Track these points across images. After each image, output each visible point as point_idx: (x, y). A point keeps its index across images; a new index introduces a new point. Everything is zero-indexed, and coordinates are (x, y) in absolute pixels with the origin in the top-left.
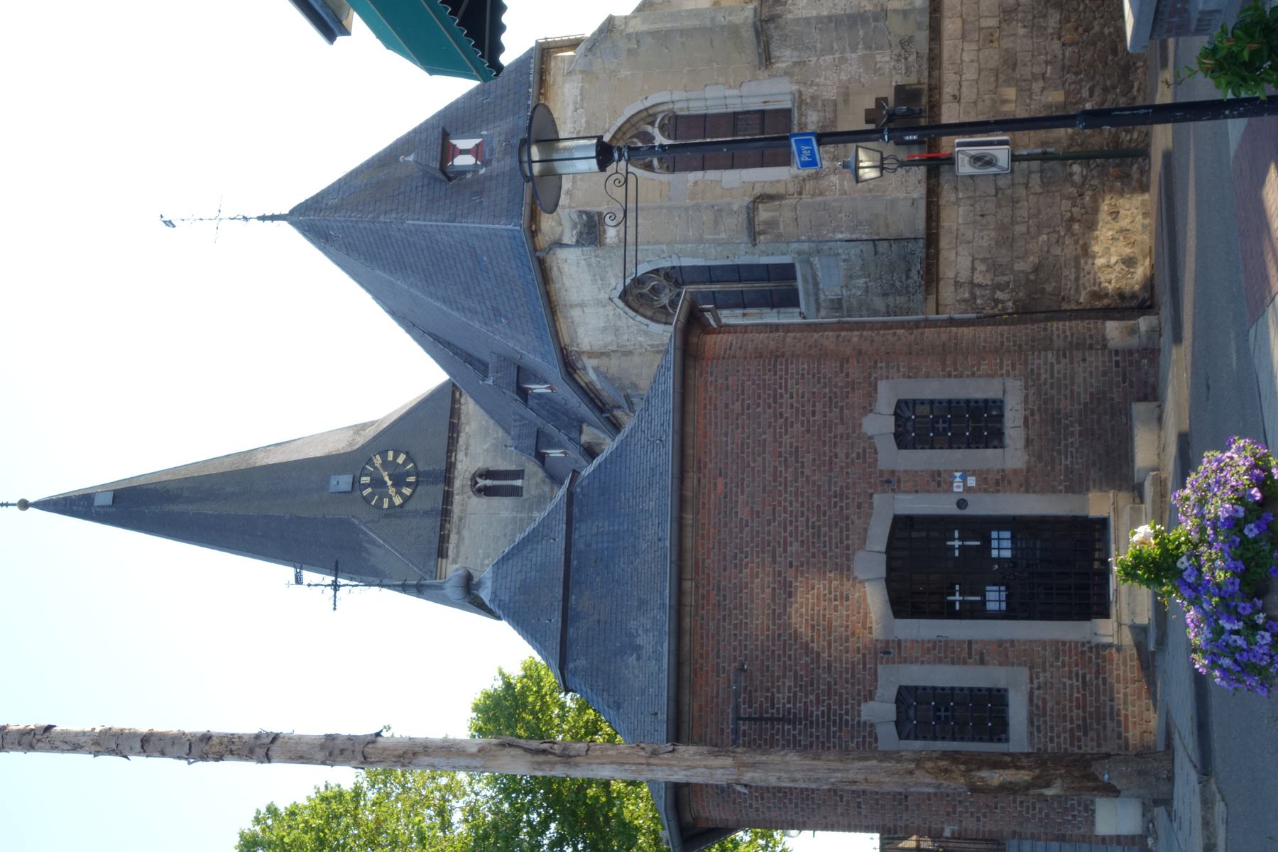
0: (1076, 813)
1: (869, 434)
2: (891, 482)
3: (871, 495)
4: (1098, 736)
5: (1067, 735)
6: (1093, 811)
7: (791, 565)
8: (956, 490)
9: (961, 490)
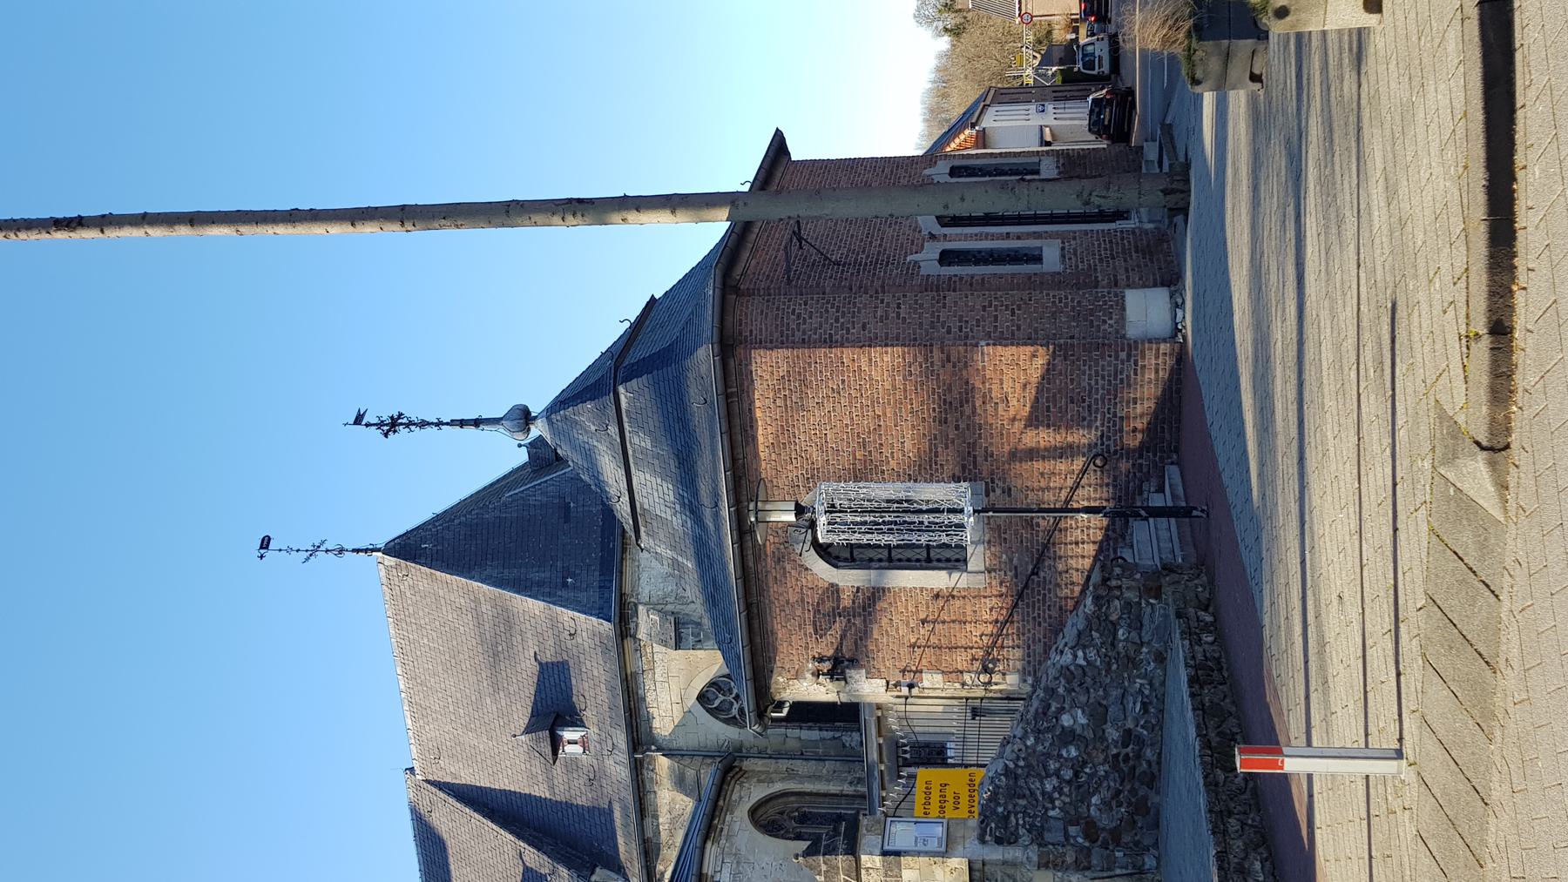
6: (1124, 297)
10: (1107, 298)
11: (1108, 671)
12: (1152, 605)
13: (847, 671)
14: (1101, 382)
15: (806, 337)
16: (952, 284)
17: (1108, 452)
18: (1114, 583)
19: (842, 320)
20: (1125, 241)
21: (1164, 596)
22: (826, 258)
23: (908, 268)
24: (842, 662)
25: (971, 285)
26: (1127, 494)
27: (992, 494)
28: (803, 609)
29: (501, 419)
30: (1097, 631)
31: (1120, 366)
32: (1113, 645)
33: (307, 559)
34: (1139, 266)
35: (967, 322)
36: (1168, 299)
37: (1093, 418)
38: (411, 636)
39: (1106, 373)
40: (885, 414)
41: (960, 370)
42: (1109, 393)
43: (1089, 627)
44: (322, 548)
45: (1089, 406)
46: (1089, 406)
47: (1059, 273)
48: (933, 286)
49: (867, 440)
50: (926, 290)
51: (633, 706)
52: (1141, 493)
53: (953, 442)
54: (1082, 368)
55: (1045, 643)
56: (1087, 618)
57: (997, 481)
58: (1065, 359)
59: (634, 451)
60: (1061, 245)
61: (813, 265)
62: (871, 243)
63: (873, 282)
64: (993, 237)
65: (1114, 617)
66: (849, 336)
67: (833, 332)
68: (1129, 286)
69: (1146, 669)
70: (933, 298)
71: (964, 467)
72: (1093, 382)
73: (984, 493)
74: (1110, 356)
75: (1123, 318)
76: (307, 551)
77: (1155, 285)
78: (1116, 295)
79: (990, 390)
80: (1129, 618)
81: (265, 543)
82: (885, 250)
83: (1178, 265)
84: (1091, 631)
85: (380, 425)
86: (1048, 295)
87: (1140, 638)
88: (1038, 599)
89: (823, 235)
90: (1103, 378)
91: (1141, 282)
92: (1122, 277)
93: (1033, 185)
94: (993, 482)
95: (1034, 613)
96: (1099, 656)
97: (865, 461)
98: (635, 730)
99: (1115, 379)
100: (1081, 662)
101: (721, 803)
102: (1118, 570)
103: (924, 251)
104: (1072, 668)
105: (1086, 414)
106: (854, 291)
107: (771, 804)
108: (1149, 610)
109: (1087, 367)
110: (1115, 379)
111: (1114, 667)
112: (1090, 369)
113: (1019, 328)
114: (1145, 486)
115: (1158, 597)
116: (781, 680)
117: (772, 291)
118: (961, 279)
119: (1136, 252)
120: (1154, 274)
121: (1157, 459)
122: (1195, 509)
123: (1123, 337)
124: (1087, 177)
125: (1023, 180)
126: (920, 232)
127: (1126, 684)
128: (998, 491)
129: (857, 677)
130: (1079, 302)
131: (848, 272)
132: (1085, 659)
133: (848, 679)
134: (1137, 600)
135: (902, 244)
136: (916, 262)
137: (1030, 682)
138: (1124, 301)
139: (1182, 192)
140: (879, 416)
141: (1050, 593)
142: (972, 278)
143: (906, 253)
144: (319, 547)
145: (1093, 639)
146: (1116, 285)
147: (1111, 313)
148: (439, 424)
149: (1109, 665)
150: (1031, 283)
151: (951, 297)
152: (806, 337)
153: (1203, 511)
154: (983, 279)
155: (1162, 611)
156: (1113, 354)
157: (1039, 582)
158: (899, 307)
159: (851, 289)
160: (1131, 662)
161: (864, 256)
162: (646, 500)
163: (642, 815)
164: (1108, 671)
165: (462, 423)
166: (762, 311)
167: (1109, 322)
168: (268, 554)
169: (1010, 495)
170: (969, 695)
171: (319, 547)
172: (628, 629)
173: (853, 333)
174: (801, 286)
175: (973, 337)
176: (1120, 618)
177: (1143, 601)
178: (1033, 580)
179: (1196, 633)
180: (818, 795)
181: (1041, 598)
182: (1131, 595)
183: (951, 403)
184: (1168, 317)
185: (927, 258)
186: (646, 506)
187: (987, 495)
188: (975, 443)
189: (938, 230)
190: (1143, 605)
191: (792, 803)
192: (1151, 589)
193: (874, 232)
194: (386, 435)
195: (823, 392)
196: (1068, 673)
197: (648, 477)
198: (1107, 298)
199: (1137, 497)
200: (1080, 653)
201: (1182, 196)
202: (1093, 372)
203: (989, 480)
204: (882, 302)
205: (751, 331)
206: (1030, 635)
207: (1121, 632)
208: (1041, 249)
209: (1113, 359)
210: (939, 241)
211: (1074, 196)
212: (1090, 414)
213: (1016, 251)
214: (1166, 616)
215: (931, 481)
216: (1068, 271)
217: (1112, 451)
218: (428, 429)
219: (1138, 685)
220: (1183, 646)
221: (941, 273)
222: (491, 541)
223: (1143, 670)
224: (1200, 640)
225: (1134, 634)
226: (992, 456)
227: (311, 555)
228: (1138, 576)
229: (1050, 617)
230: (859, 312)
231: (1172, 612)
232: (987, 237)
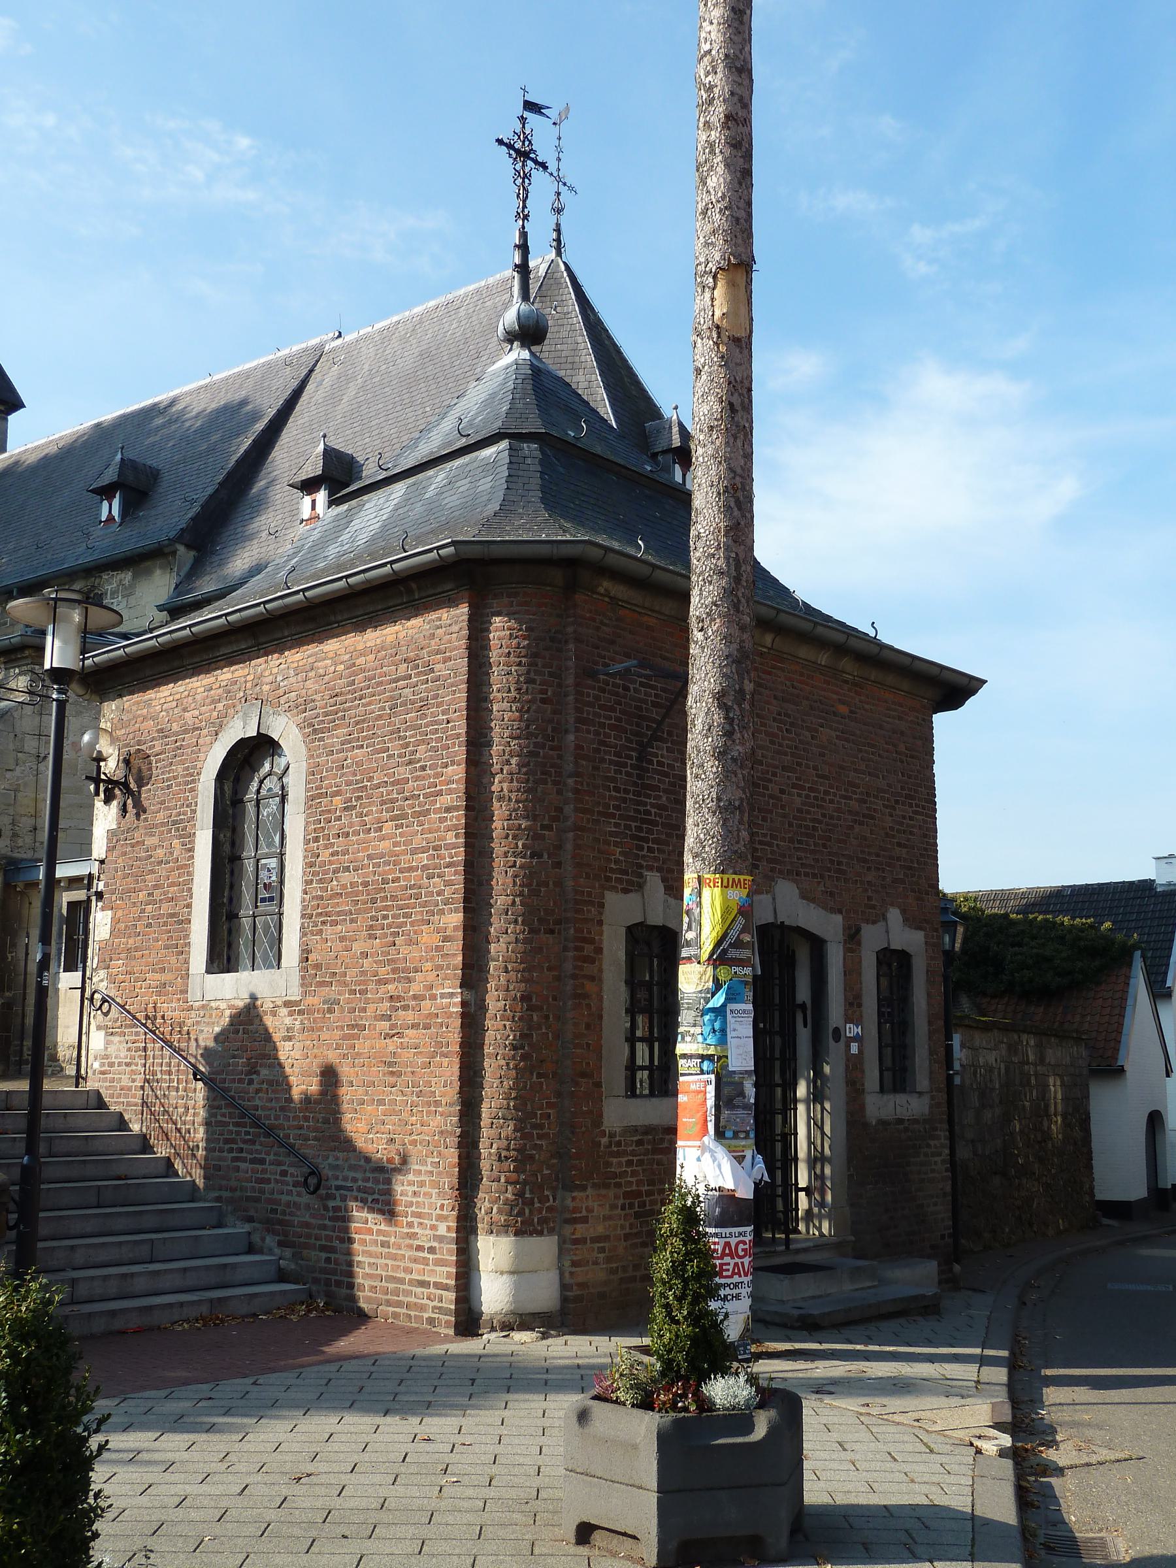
0: (537, 1205)
1: (889, 915)
2: (852, 937)
3: (840, 912)
4: (636, 1235)
5: (634, 1188)
6: (540, 1233)
7: (782, 792)
8: (848, 1026)
9: (848, 1035)
14: (410, 1189)
37: (368, 1175)
40: (382, 839)
54: (429, 1160)
58: (441, 1132)
71: (318, 966)
73: (288, 998)
74: (442, 1206)
77: (564, 1287)
79: (405, 1008)
86: (550, 1105)
92: (581, 1230)
94: (301, 1012)
97: (329, 811)
109: (429, 1168)
128: (288, 1021)
130: (532, 1157)
140: (380, 829)
142: (592, 978)
156: (445, 1213)
187: (287, 1004)
188: (345, 984)
195: (412, 736)
198: (537, 1205)
215: (303, 916)
221: (605, 927)
226: (330, 1011)
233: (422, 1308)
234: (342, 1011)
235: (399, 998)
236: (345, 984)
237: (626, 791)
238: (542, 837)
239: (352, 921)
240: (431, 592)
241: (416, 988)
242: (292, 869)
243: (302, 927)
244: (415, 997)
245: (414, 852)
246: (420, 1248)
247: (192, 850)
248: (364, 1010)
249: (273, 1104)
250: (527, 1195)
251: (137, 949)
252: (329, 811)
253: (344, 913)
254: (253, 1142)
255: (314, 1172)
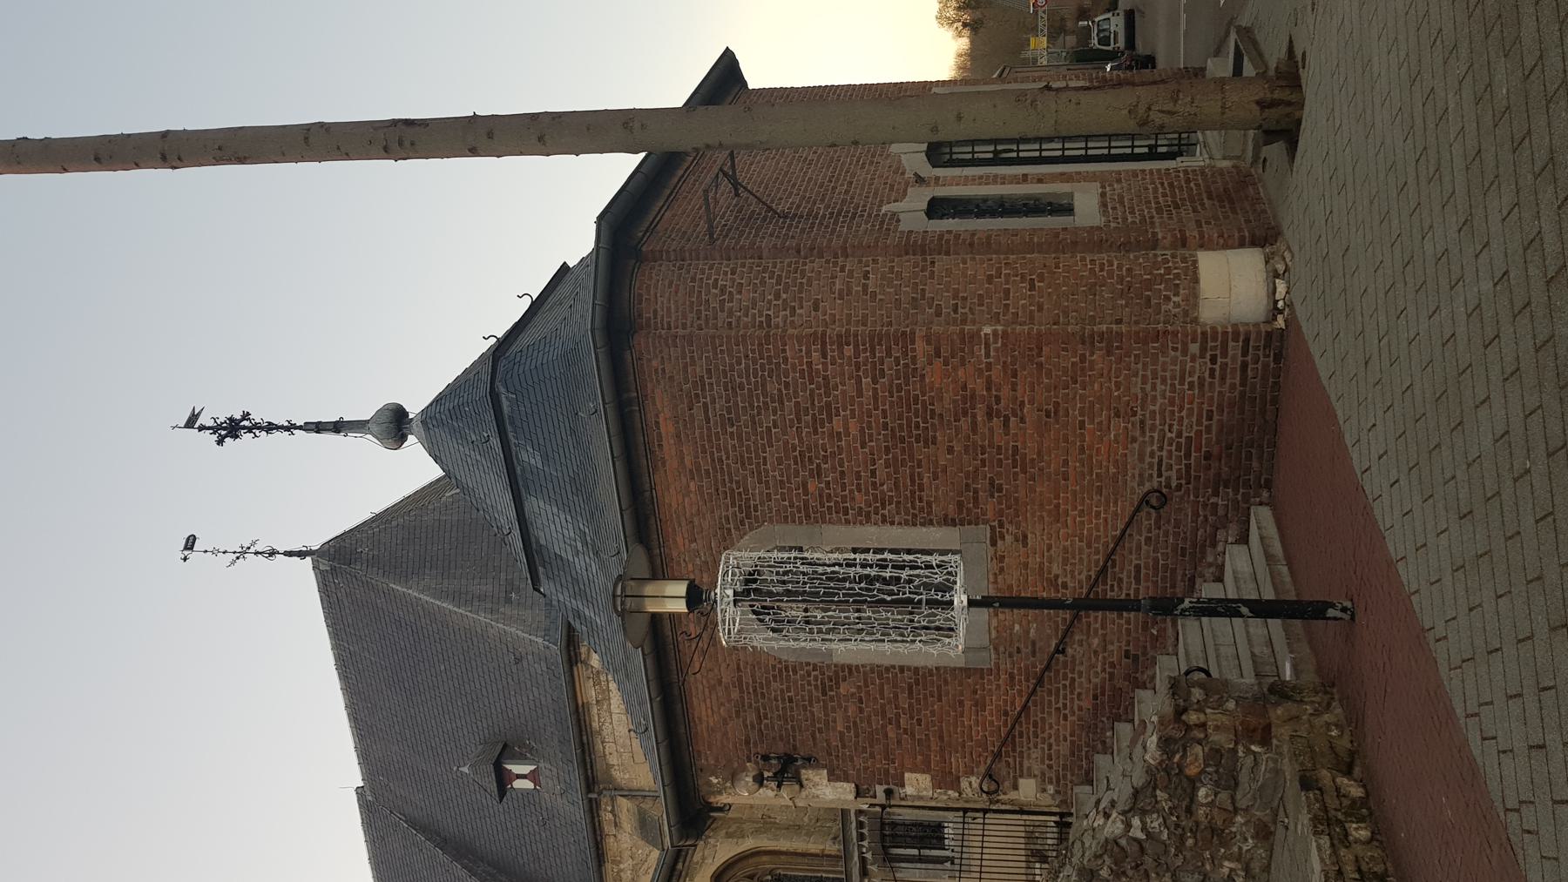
6: (1195, 262)
10: (1170, 264)
11: (1180, 848)
12: (1254, 753)
13: (803, 771)
14: (1160, 387)
15: (733, 320)
16: (944, 245)
17: (1168, 486)
18: (1193, 717)
19: (784, 296)
20: (1192, 185)
21: (1275, 742)
22: (770, 209)
23: (882, 223)
24: (796, 760)
25: (971, 245)
26: (1194, 545)
27: (1000, 543)
28: (742, 691)
29: (367, 422)
30: (1164, 789)
31: (1189, 365)
32: (1189, 811)
33: (233, 562)
34: (1216, 218)
35: (964, 299)
36: (1262, 266)
37: (1147, 439)
38: (351, 648)
39: (1168, 374)
41: (955, 369)
42: (1172, 403)
43: (1152, 784)
44: (252, 550)
45: (1142, 422)
46: (1142, 422)
47: (1099, 228)
48: (917, 247)
49: (823, 466)
50: (907, 254)
51: (585, 741)
52: (1214, 545)
53: (945, 470)
55: (1072, 743)
56: (1149, 770)
57: (1006, 526)
58: (1109, 353)
59: (523, 470)
60: (1100, 190)
61: (750, 218)
62: (834, 188)
63: (830, 241)
64: (1004, 180)
65: (1192, 771)
66: (796, 318)
67: (771, 313)
68: (1202, 246)
69: (1240, 848)
70: (916, 265)
71: (960, 505)
72: (1148, 387)
73: (988, 542)
74: (1175, 349)
75: (1194, 296)
76: (234, 553)
77: (1242, 245)
78: (1184, 260)
80: (1217, 772)
81: (190, 543)
82: (852, 198)
83: (1275, 217)
84: (1154, 789)
85: (215, 429)
86: (1083, 259)
87: (1233, 803)
88: (1065, 686)
89: (770, 178)
90: (1164, 381)
91: (1221, 241)
92: (1192, 233)
93: (1064, 96)
94: (1001, 525)
95: (1057, 703)
96: (1166, 827)
98: (589, 767)
99: (1182, 383)
100: (1137, 833)
101: (680, 866)
102: (1197, 694)
103: (907, 199)
104: (1123, 842)
105: (1138, 433)
106: (802, 253)
107: (740, 865)
108: (1249, 761)
109: (1140, 366)
110: (1182, 383)
111: (1190, 842)
112: (1144, 370)
113: (1040, 309)
114: (1220, 535)
115: (1265, 741)
116: (715, 781)
117: (687, 254)
118: (957, 236)
119: (1209, 198)
120: (1240, 230)
121: (1239, 497)
122: (1333, 606)
123: (1195, 320)
124: (1143, 84)
125: (1048, 88)
126: (903, 174)
127: (1208, 867)
129: (817, 779)
130: (1128, 270)
131: (797, 227)
132: (1144, 829)
133: (805, 782)
134: (1231, 746)
135: (877, 191)
136: (894, 214)
137: (1052, 792)
138: (1197, 268)
139: (1289, 104)
141: (1080, 677)
143: (882, 201)
144: (249, 548)
145: (1157, 802)
146: (1184, 245)
147: (1178, 285)
148: (290, 428)
149: (1182, 839)
150: (1059, 244)
151: (942, 262)
152: (733, 320)
153: (1344, 610)
154: (989, 237)
155: (1271, 765)
156: (1179, 346)
157: (1065, 663)
158: (866, 277)
159: (798, 252)
160: (1217, 835)
161: (822, 206)
162: (541, 534)
163: (599, 861)
164: (1180, 848)
165: (319, 428)
166: (671, 283)
167: (1175, 299)
168: (192, 556)
169: (1025, 545)
170: (967, 806)
171: (249, 548)
172: (578, 655)
173: (801, 315)
174: (728, 246)
175: (974, 322)
176: (1203, 772)
177: (1241, 749)
178: (1058, 659)
179: (1339, 822)
180: (795, 854)
181: (1068, 683)
182: (1222, 739)
183: (941, 415)
184: (1262, 292)
185: (911, 209)
186: (543, 542)
187: (994, 543)
189: (927, 171)
190: (1241, 754)
191: (764, 863)
192: (1254, 730)
193: (840, 174)
194: (220, 442)
195: (758, 401)
196: (1116, 849)
197: (542, 504)
198: (1170, 264)
199: (1209, 550)
200: (1136, 822)
201: (1288, 110)
202: (1149, 373)
203: (996, 523)
204: (842, 270)
205: (655, 312)
206: (1053, 732)
207: (1202, 792)
208: (1071, 195)
209: (1179, 353)
210: (928, 185)
211: (1125, 112)
212: (1143, 433)
213: (1036, 198)
214: (1277, 772)
215: (914, 525)
216: (1113, 225)
217: (1174, 484)
218: (277, 434)
219: (1226, 871)
220: (1319, 848)
222: (429, 548)
223: (1236, 849)
224: (1346, 835)
225: (1224, 796)
226: (1000, 490)
227: (238, 558)
228: (1231, 705)
229: (1080, 709)
230: (810, 284)
231: (1289, 769)
232: (995, 179)
233: (1266, 366)
234: (999, 474)
235: (989, 407)
236: (977, 470)
237: (813, 223)
238: (851, 272)
239: (919, 466)
240: (632, 378)
241: (978, 385)
242: (871, 540)
243: (923, 525)
244: (989, 389)
245: (860, 394)
246: (1212, 371)
247: (850, 667)
248: (999, 447)
249: (1084, 556)
250: (1162, 272)
251: (941, 738)
252: (821, 496)
253: (912, 476)
254: (1121, 580)
255: (1144, 500)
